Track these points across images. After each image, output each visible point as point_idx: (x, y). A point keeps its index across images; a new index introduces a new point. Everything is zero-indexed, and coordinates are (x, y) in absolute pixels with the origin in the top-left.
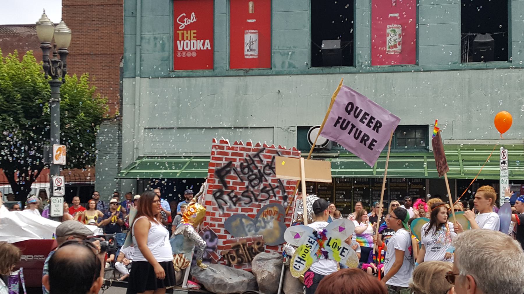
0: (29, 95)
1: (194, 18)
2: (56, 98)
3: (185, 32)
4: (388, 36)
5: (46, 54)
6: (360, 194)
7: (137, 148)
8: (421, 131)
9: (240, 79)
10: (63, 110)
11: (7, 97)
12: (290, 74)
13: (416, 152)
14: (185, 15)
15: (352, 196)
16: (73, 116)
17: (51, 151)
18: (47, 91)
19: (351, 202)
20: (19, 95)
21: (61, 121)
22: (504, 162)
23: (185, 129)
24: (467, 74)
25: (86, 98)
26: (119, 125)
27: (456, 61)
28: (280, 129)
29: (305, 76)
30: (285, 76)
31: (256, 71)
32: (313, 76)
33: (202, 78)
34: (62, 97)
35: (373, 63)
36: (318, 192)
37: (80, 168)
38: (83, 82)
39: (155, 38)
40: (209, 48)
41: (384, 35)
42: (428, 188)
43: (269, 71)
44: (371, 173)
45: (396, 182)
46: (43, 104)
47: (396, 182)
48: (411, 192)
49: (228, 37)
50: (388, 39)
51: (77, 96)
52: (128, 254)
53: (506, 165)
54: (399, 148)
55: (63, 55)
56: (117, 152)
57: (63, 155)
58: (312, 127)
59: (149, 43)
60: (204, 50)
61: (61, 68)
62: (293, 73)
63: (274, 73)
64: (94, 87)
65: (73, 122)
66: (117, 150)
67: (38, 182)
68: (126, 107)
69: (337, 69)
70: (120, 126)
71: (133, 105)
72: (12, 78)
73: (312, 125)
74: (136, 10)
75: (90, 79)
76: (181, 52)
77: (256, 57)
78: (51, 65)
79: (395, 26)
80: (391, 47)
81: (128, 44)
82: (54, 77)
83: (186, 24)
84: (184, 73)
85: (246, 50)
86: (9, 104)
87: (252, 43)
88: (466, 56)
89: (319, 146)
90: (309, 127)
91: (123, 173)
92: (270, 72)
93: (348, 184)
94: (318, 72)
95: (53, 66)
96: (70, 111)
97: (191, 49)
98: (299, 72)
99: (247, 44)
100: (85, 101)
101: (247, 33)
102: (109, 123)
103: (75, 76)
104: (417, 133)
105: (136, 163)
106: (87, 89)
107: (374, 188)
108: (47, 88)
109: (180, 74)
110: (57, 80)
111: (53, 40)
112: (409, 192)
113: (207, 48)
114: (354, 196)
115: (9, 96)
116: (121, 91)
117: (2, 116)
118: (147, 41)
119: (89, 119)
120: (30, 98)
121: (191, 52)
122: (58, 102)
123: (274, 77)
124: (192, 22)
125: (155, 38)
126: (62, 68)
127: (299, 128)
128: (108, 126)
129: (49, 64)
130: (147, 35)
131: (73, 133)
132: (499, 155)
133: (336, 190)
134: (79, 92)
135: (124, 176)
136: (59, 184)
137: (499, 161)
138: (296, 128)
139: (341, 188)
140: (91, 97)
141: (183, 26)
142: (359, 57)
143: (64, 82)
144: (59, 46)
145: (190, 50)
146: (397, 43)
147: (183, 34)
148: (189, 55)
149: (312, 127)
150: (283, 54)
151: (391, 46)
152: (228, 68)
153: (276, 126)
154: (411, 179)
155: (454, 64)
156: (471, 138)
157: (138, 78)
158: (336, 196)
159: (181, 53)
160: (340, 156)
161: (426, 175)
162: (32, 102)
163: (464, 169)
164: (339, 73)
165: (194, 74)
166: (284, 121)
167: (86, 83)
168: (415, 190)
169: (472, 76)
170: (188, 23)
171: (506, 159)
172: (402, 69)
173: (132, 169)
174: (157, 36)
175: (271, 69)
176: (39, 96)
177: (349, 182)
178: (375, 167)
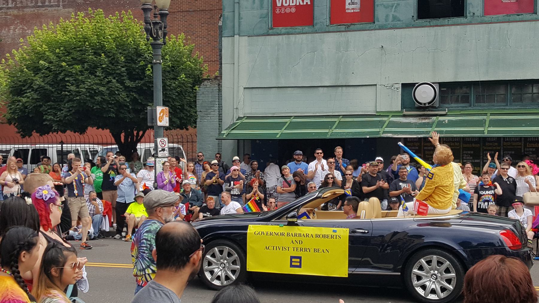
0: (133, 57)
2: (158, 60)
5: (146, 16)
6: (470, 154)
7: (236, 109)
9: (341, 36)
10: (164, 71)
11: (112, 59)
13: (533, 108)
16: (175, 77)
17: (154, 112)
18: (149, 53)
20: (122, 58)
21: (162, 82)
23: (284, 88)
25: (187, 58)
26: (219, 85)
29: (410, 29)
31: (358, 26)
33: (301, 35)
34: (163, 58)
35: (486, 12)
36: (424, 153)
37: (182, 129)
40: (309, 3)
44: (483, 132)
46: (146, 66)
47: (510, 141)
48: (527, 151)
54: (513, 104)
55: (163, 16)
56: (218, 113)
60: (303, 5)
61: (162, 30)
62: (398, 26)
65: (175, 83)
66: (218, 110)
67: (143, 142)
68: (226, 68)
69: (446, 21)
70: (220, 85)
72: (115, 40)
73: (418, 82)
77: (358, 11)
78: (152, 26)
82: (155, 39)
85: (347, 3)
86: (113, 67)
89: (425, 104)
90: (414, 84)
91: (224, 133)
92: (373, 27)
93: (456, 144)
94: (425, 24)
96: (171, 72)
97: (290, 5)
100: (185, 62)
102: (209, 84)
104: (534, 88)
105: (236, 123)
107: (485, 148)
108: (149, 50)
109: (279, 31)
112: (524, 151)
113: (307, 3)
114: (463, 157)
115: (114, 58)
116: (221, 51)
117: (108, 79)
119: (190, 80)
120: (133, 60)
121: (291, 8)
122: (160, 64)
126: (163, 29)
127: (404, 85)
131: (174, 94)
135: (224, 136)
136: (163, 145)
138: (401, 85)
142: (471, 6)
143: (165, 43)
144: (160, 7)
148: (288, 11)
150: (386, 7)
153: (379, 84)
157: (236, 37)
159: (280, 9)
160: (448, 114)
162: (135, 63)
164: (448, 25)
165: (294, 31)
168: (531, 149)
173: (232, 130)
175: (374, 23)
176: (141, 57)
178: (487, 126)
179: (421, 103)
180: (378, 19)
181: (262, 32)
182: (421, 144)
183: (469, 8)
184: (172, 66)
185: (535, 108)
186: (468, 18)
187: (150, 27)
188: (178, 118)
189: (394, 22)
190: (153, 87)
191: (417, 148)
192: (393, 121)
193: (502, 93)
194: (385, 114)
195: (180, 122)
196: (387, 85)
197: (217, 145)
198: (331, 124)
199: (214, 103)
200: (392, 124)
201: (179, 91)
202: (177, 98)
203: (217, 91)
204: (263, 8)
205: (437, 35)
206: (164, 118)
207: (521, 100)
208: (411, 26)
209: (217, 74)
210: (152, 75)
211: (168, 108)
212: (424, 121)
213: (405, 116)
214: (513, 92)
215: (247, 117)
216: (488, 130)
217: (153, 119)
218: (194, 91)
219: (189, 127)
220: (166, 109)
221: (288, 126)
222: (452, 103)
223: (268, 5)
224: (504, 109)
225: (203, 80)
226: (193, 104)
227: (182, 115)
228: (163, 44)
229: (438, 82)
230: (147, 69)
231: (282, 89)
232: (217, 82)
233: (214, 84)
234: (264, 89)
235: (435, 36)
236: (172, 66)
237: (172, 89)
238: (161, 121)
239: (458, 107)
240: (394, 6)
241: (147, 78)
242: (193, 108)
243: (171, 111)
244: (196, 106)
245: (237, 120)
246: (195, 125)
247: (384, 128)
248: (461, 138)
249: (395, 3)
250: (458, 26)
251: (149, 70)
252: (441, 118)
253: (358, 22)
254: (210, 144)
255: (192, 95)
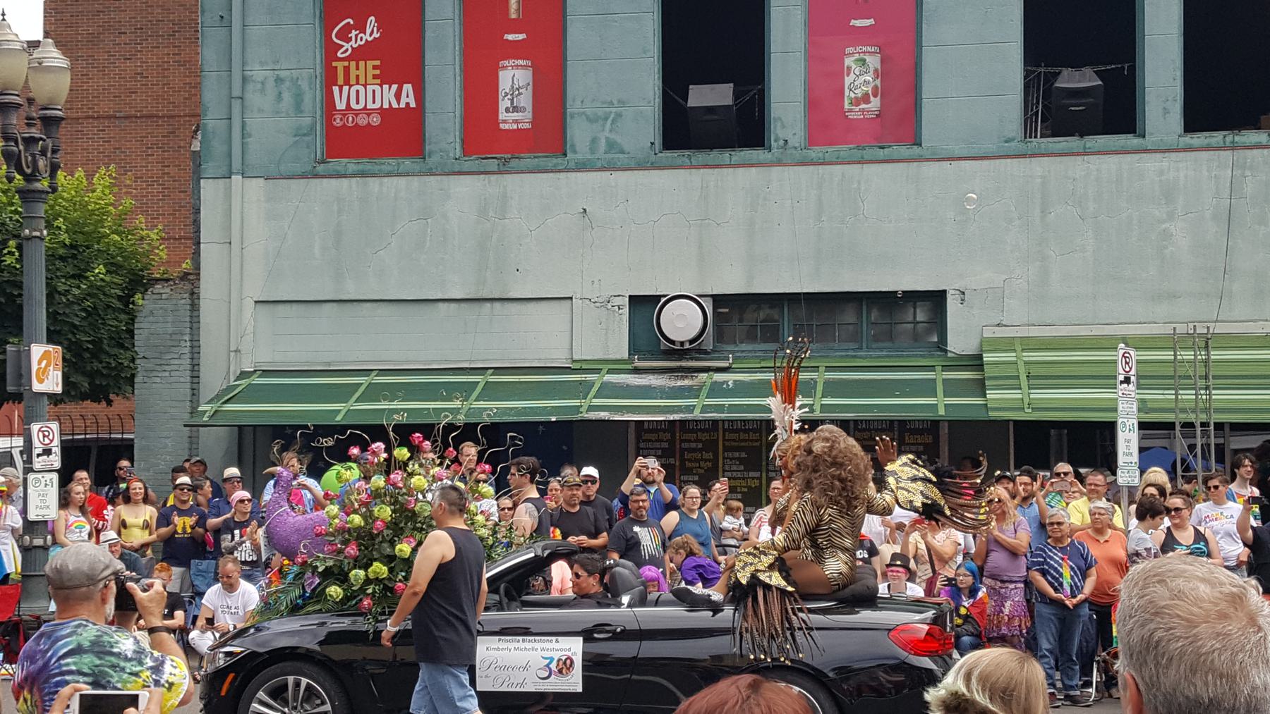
1: (375, 29)
3: (353, 64)
4: (848, 75)
5: (6, 122)
7: (236, 351)
8: (928, 303)
9: (489, 182)
10: (51, 257)
12: (610, 167)
14: (352, 22)
15: (764, 463)
17: (23, 359)
18: (12, 212)
19: (760, 479)
21: (47, 284)
22: (1127, 380)
23: (355, 303)
24: (1039, 167)
26: (192, 294)
27: (1012, 135)
28: (588, 302)
30: (599, 173)
31: (528, 161)
32: (666, 172)
34: (49, 225)
35: (813, 139)
36: (682, 456)
38: (100, 189)
39: (279, 80)
40: (413, 105)
41: (839, 73)
42: (947, 442)
43: (559, 160)
45: (870, 430)
47: (870, 430)
49: (458, 78)
50: (848, 80)
51: (85, 224)
52: (220, 610)
53: (1131, 386)
55: (50, 123)
56: (188, 361)
57: (54, 370)
58: (665, 296)
59: (263, 91)
60: (399, 109)
61: (46, 157)
63: (572, 165)
64: (128, 202)
65: (79, 287)
66: (188, 356)
69: (725, 156)
70: (194, 295)
71: (228, 245)
73: (665, 293)
74: (231, 10)
75: (116, 184)
76: (344, 114)
77: (528, 126)
78: (21, 147)
79: (864, 49)
80: (856, 102)
81: (212, 94)
82: (29, 178)
83: (355, 46)
84: (350, 164)
87: (517, 92)
88: (1036, 122)
89: (682, 343)
90: (659, 297)
92: (562, 164)
93: (753, 436)
94: (679, 162)
95: (26, 150)
97: (368, 107)
98: (632, 165)
99: (506, 94)
100: (107, 236)
101: (504, 68)
103: (80, 173)
104: (918, 311)
106: (111, 204)
108: (12, 204)
109: (340, 168)
110: (38, 186)
111: (26, 86)
113: (408, 104)
116: (198, 211)
118: (259, 86)
119: (117, 280)
121: (369, 115)
122: (41, 239)
123: (573, 175)
124: (370, 39)
125: (279, 80)
126: (49, 155)
127: (636, 302)
128: (164, 296)
129: (18, 147)
130: (258, 73)
131: (77, 316)
132: (1115, 362)
133: (724, 451)
134: (92, 213)
136: (47, 441)
137: (1115, 377)
138: (627, 299)
139: (736, 444)
140: (120, 226)
141: (347, 50)
142: (779, 124)
143: (54, 190)
144: (41, 99)
145: (365, 108)
146: (870, 92)
147: (347, 69)
148: (362, 120)
149: (665, 296)
150: (592, 120)
151: (856, 98)
152: (458, 153)
153: (578, 296)
154: (905, 421)
155: (1006, 142)
156: (1049, 322)
157: (236, 178)
158: (724, 464)
159: (345, 115)
161: (942, 412)
163: (1032, 396)
165: (377, 168)
166: (596, 282)
167: (107, 191)
169: (1049, 171)
170: (359, 42)
171: (1133, 372)
172: (881, 154)
174: (283, 74)
175: (565, 155)
177: (754, 431)
178: (819, 394)
179: (673, 342)
180: (573, 146)
181: (298, 168)
182: (673, 435)
183: (775, 128)
184: (72, 246)
185: (921, 356)
186: (773, 151)
187: (15, 149)
188: (84, 374)
189: (610, 156)
190: (20, 295)
191: (666, 445)
192: (612, 383)
193: (851, 321)
194: (593, 367)
195: (89, 384)
196: (596, 300)
197: (186, 439)
198: (467, 389)
199: (178, 337)
200: (608, 390)
201: (89, 306)
202: (85, 323)
203: (188, 307)
204: (301, 112)
205: (707, 187)
206: (51, 373)
207: (890, 337)
208: (649, 165)
209: (187, 265)
210: (18, 266)
211: (60, 347)
212: (679, 383)
213: (637, 371)
214: (873, 318)
215: (263, 371)
216: (822, 405)
217: (20, 376)
218: (131, 306)
219: (112, 396)
220: (56, 351)
221: (363, 392)
222: (742, 342)
223: (314, 107)
224: (855, 357)
225: (151, 282)
226: (125, 338)
227: (96, 365)
228: (50, 190)
229: (711, 293)
230: (5, 251)
231: (349, 305)
232: (188, 287)
233: (179, 291)
234: (302, 306)
235: (702, 188)
236: (71, 245)
237: (73, 302)
238: (41, 381)
239: (755, 351)
240: (609, 122)
241: (5, 274)
242: (127, 349)
243: (68, 357)
244: (134, 346)
245: (238, 379)
246: (129, 389)
247: (591, 399)
248: (764, 423)
249: (611, 112)
250: (753, 168)
251: (10, 253)
252: (719, 377)
253: (529, 152)
254: (169, 438)
255: (123, 316)
